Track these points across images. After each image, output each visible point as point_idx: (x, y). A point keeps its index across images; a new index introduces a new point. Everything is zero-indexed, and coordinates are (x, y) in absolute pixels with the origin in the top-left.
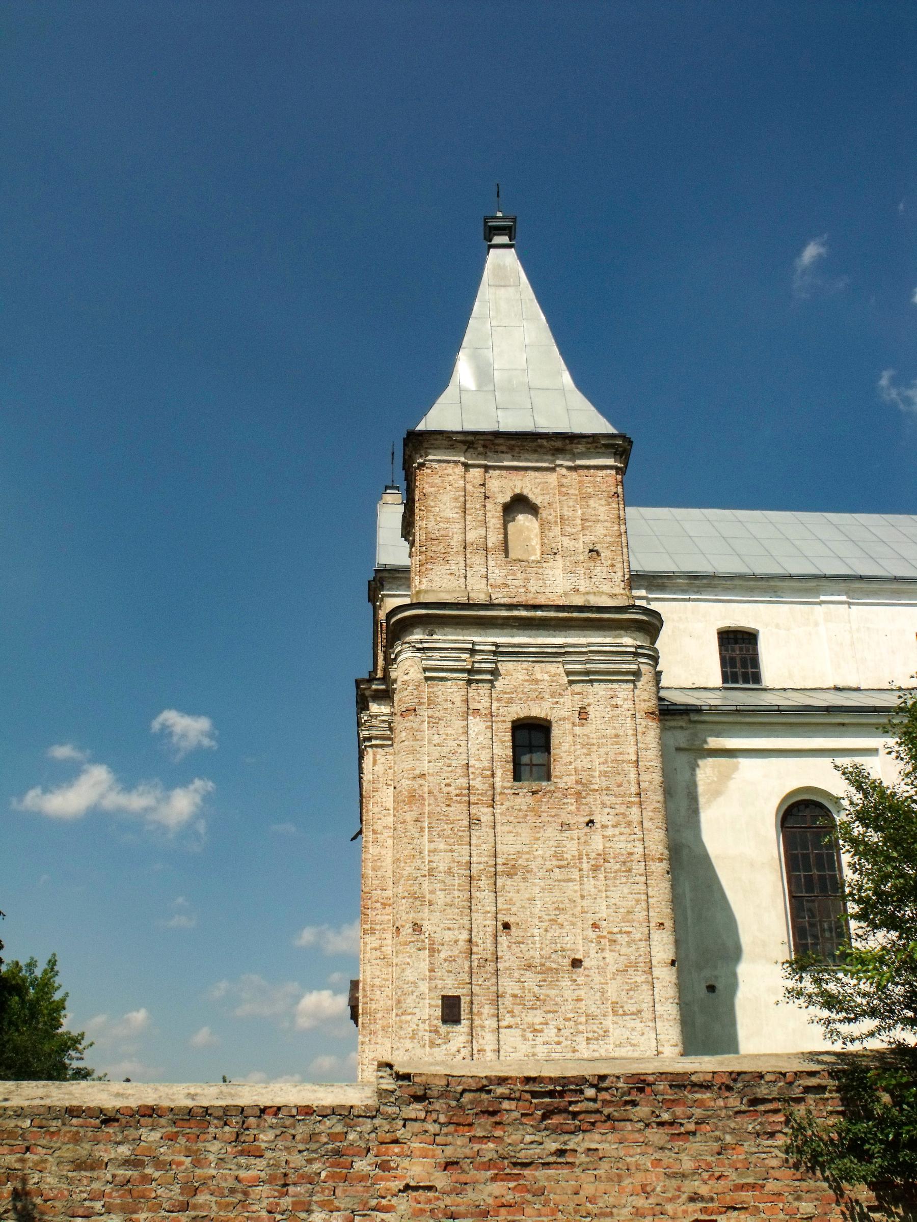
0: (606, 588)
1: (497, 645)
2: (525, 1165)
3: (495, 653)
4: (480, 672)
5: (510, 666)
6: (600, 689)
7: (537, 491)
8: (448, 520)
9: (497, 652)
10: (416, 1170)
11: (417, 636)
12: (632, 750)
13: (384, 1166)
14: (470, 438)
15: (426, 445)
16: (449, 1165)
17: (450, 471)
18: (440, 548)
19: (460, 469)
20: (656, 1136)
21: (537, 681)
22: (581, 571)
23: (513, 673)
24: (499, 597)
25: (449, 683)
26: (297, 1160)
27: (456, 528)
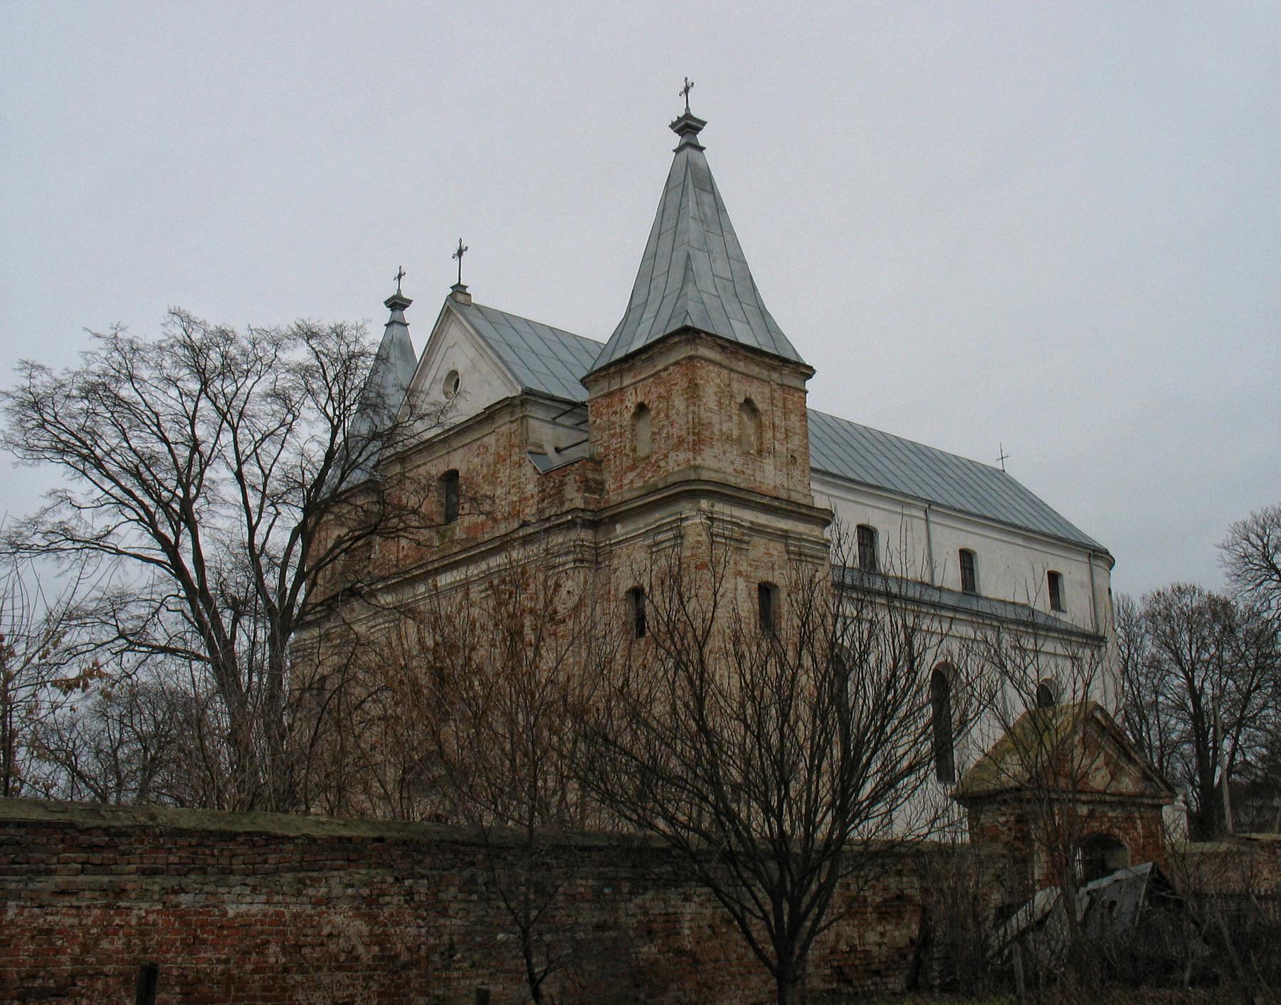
1: (751, 522)
3: (750, 529)
9: (756, 529)
11: (704, 504)
18: (708, 433)
21: (771, 555)
22: (785, 470)
23: (759, 547)
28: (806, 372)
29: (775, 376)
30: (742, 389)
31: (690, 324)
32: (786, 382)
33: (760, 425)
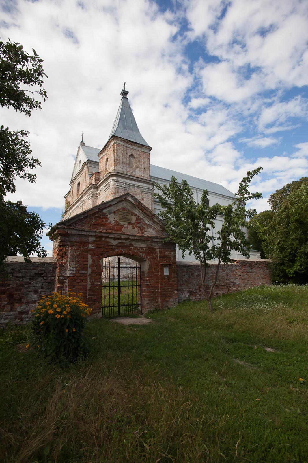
0: (146, 176)
1: (129, 183)
2: (248, 273)
4: (126, 188)
5: (131, 188)
6: (145, 195)
7: (135, 154)
8: (120, 156)
9: (129, 184)
10: (239, 273)
12: (151, 207)
13: (236, 273)
14: (125, 140)
15: (116, 139)
16: (242, 273)
17: (120, 146)
19: (122, 146)
20: (258, 269)
21: (135, 192)
24: (128, 174)
25: (121, 189)
26: (228, 272)
27: (121, 158)
28: (150, 149)
29: (140, 149)
30: (130, 152)
31: (115, 135)
32: (144, 151)
33: (136, 161)
